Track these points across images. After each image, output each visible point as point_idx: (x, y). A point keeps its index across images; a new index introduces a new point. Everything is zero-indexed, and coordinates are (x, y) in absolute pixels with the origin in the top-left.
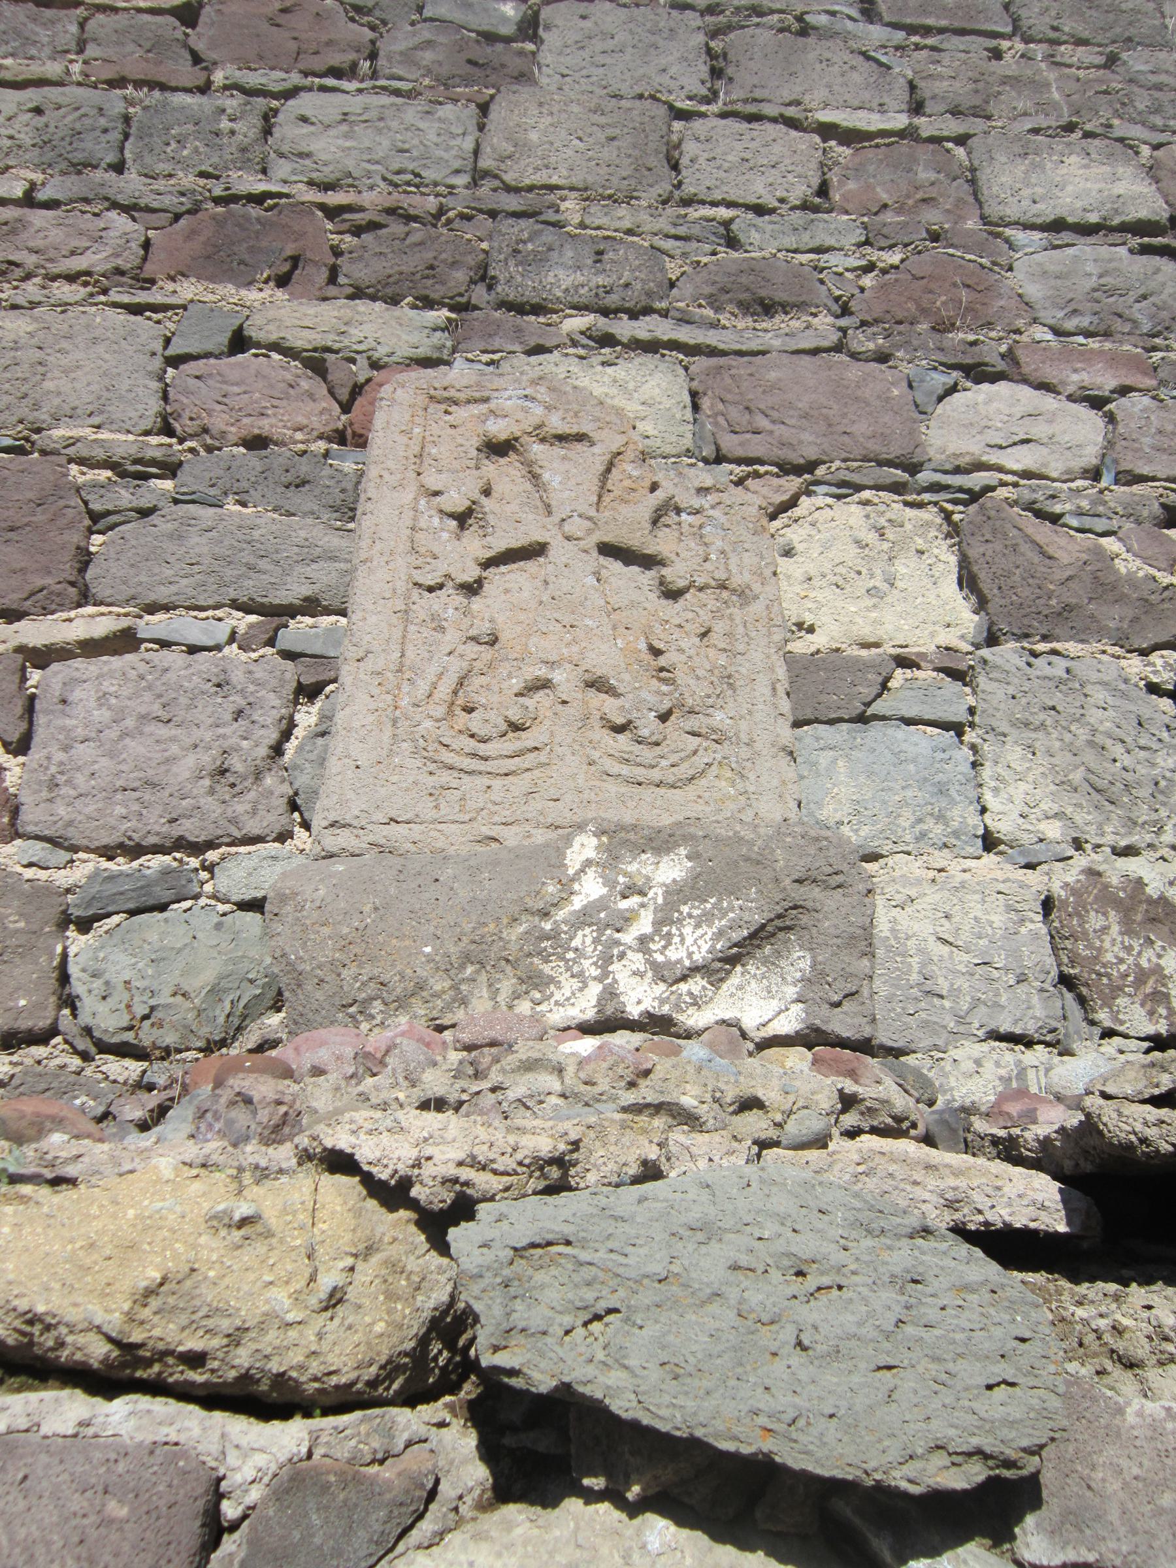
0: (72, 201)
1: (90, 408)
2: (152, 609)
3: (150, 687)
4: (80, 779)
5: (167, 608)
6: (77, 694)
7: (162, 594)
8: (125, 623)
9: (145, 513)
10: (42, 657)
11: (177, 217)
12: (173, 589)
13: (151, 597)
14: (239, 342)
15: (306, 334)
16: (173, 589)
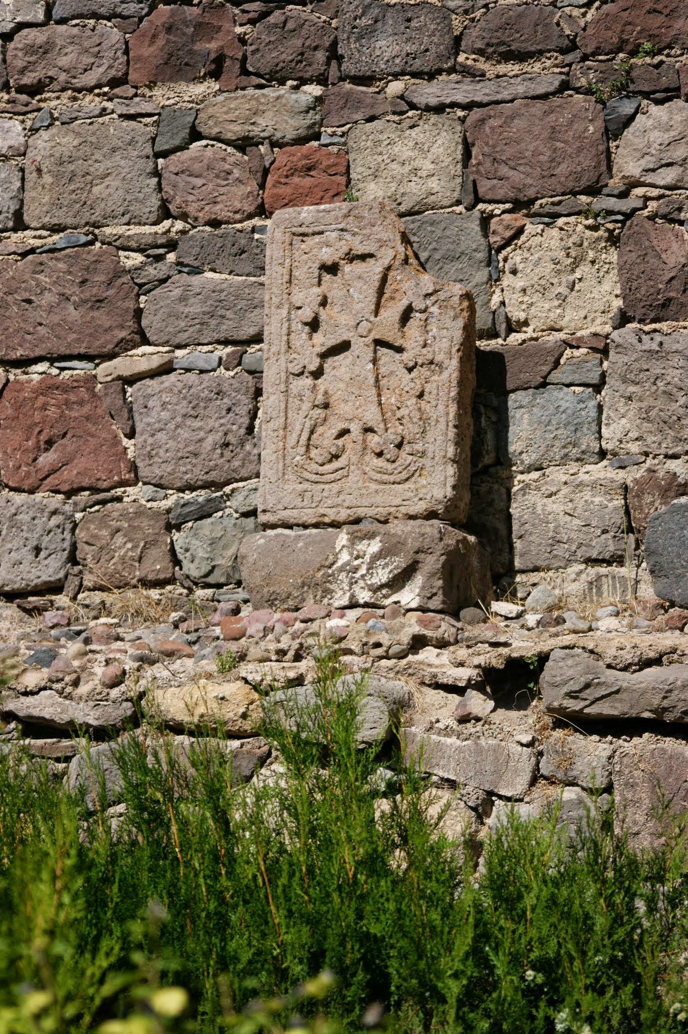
0: (74, 17)
1: (122, 210)
2: (179, 347)
3: (185, 398)
4: (162, 452)
5: (185, 346)
6: (150, 404)
7: (182, 338)
8: (167, 357)
9: (163, 281)
10: (131, 380)
11: (141, 20)
12: (186, 335)
13: (177, 341)
14: (195, 135)
15: (232, 127)
16: (186, 335)
